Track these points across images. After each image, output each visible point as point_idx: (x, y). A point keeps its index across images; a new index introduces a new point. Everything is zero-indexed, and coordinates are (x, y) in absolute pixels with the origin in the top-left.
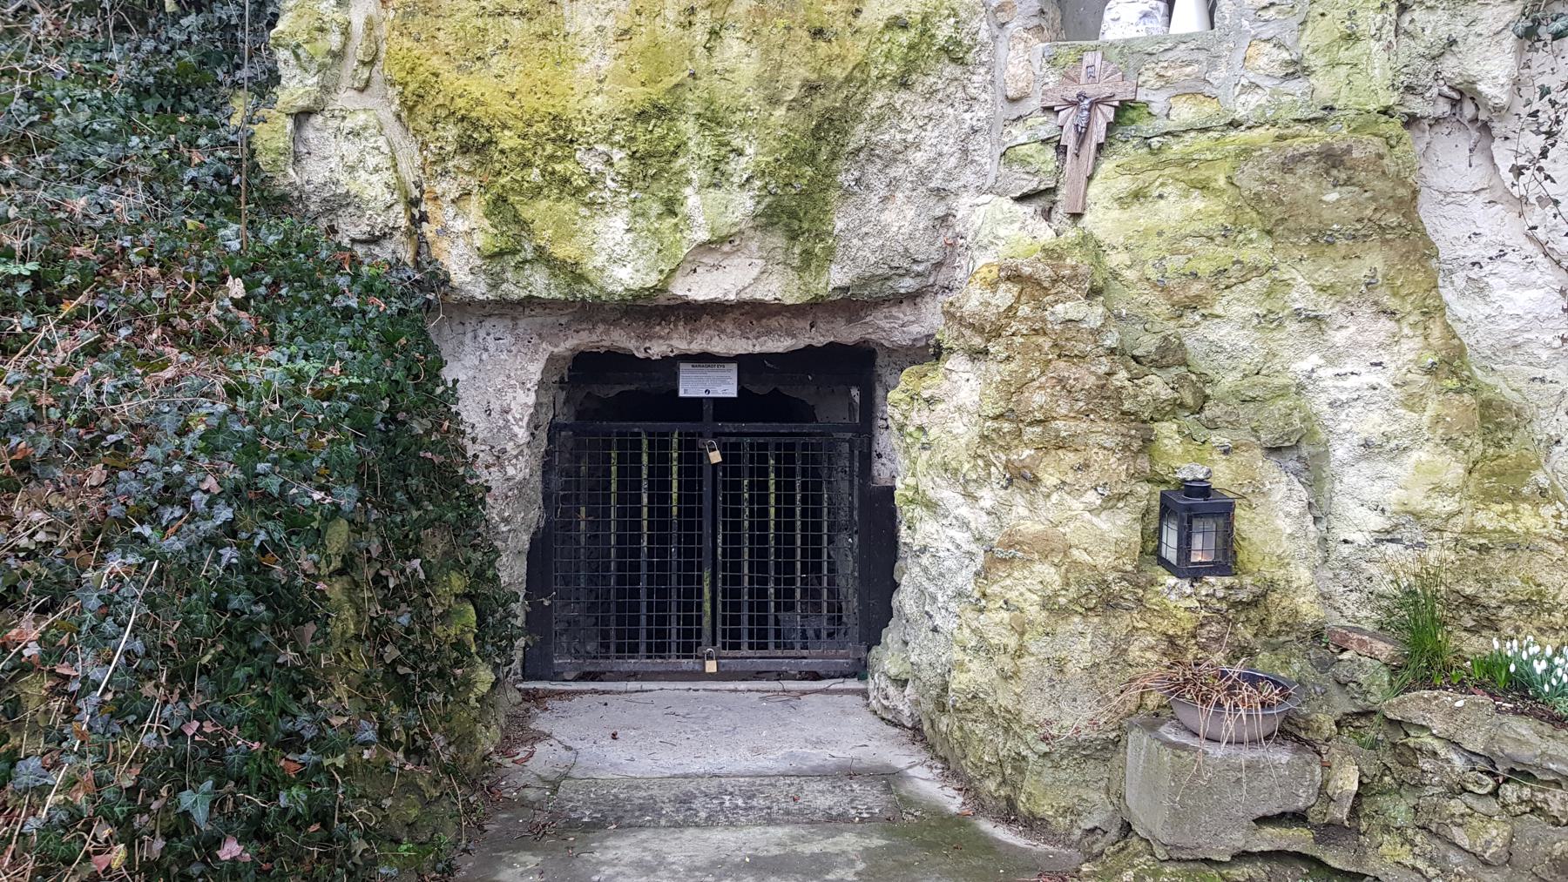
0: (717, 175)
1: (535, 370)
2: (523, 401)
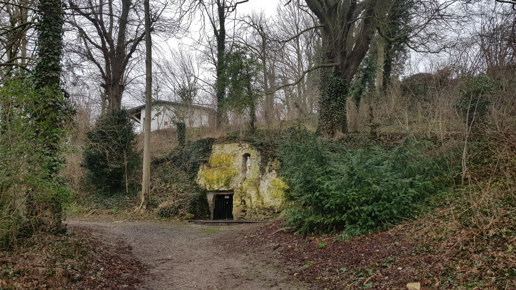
0: (222, 182)
1: (213, 196)
2: (212, 198)
